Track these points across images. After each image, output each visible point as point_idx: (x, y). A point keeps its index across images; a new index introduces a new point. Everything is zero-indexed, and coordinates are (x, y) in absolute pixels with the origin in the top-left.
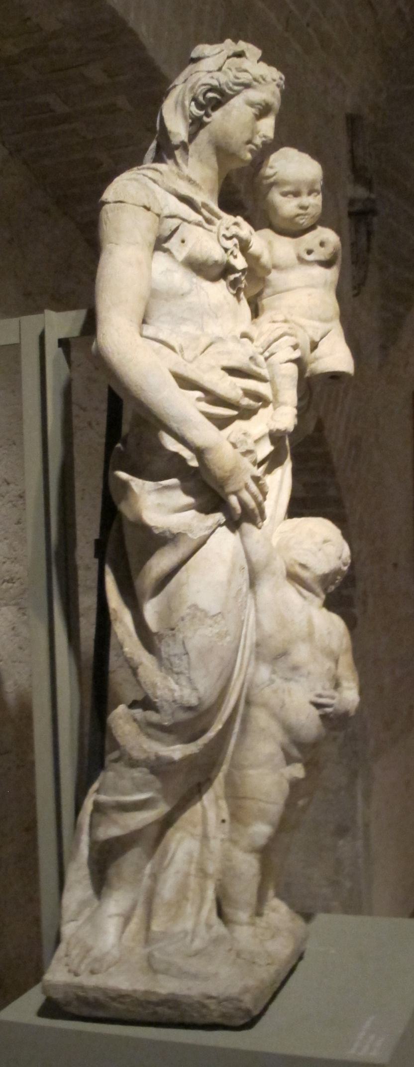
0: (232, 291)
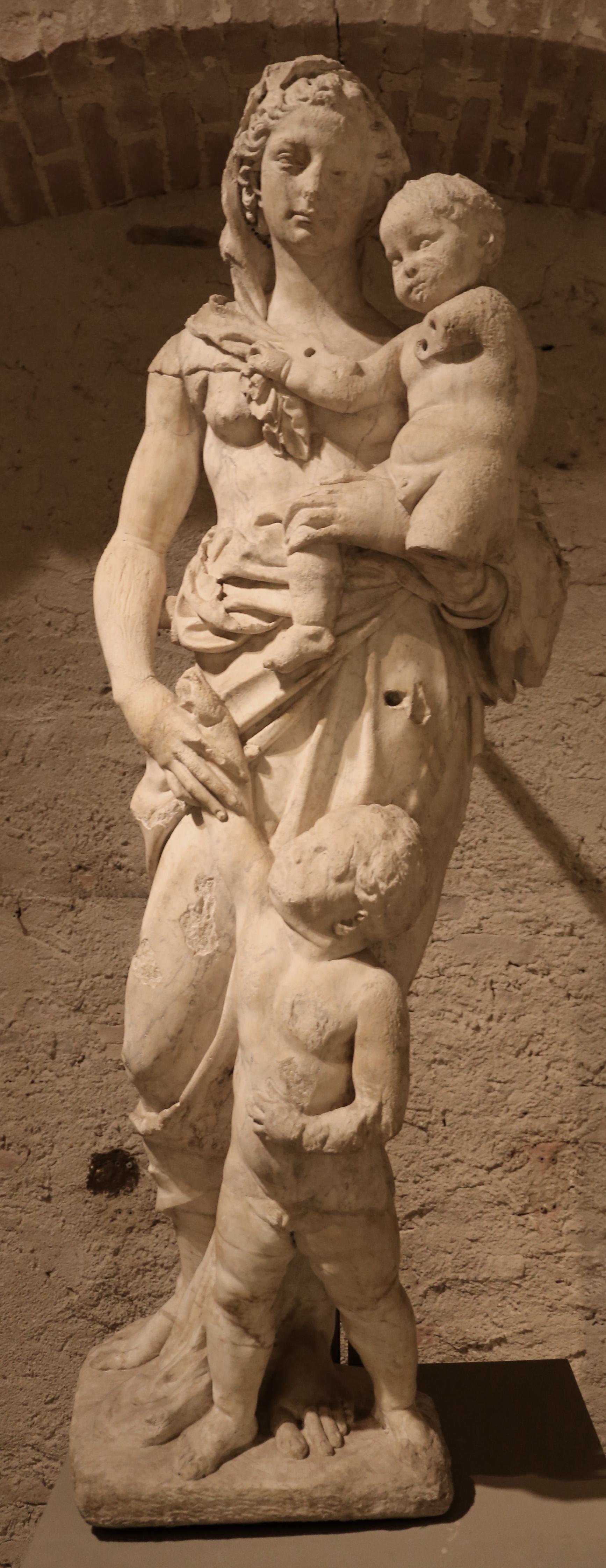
0: (277, 452)
